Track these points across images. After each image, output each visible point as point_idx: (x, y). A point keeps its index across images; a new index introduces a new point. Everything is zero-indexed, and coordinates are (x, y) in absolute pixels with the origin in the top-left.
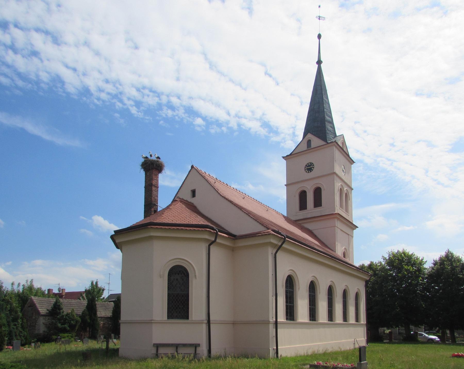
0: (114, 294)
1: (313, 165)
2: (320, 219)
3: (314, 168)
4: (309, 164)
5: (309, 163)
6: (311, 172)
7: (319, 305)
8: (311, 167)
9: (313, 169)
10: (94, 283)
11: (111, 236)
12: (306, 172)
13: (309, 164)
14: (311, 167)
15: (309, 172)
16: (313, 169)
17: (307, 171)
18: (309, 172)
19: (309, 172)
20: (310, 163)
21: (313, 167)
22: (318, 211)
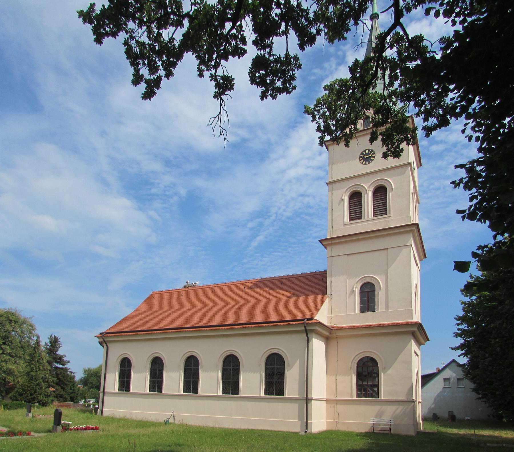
0: (131, 314)
1: (374, 153)
2: (389, 232)
3: (374, 157)
4: (367, 152)
5: (367, 150)
6: (369, 163)
7: (426, 387)
8: (370, 155)
9: (372, 158)
10: (182, 27)
11: (183, 34)
12: (362, 163)
13: (367, 152)
14: (370, 155)
15: (367, 163)
16: (372, 158)
17: (363, 162)
18: (366, 164)
19: (367, 163)
20: (369, 150)
21: (373, 155)
22: (381, 223)
